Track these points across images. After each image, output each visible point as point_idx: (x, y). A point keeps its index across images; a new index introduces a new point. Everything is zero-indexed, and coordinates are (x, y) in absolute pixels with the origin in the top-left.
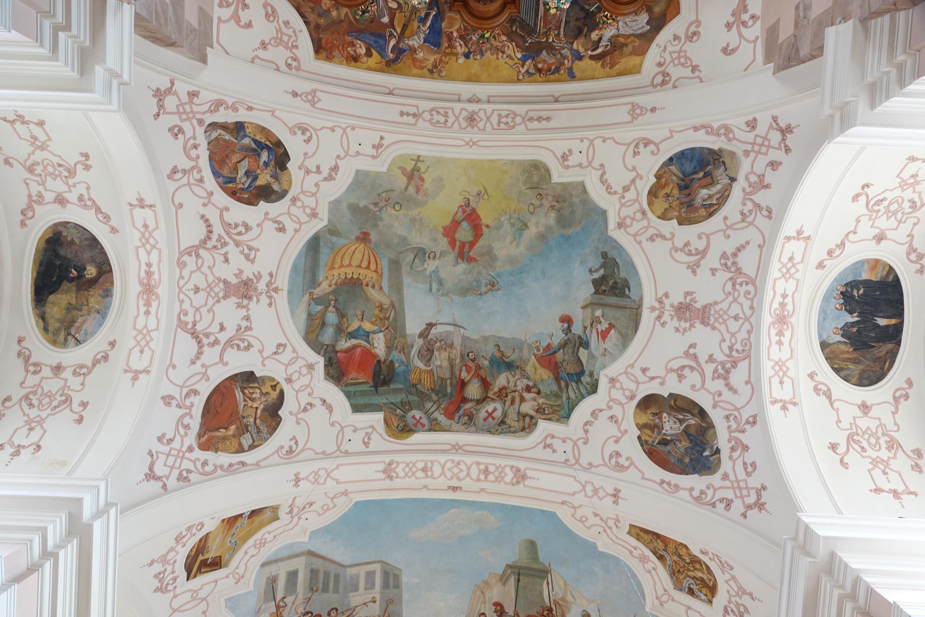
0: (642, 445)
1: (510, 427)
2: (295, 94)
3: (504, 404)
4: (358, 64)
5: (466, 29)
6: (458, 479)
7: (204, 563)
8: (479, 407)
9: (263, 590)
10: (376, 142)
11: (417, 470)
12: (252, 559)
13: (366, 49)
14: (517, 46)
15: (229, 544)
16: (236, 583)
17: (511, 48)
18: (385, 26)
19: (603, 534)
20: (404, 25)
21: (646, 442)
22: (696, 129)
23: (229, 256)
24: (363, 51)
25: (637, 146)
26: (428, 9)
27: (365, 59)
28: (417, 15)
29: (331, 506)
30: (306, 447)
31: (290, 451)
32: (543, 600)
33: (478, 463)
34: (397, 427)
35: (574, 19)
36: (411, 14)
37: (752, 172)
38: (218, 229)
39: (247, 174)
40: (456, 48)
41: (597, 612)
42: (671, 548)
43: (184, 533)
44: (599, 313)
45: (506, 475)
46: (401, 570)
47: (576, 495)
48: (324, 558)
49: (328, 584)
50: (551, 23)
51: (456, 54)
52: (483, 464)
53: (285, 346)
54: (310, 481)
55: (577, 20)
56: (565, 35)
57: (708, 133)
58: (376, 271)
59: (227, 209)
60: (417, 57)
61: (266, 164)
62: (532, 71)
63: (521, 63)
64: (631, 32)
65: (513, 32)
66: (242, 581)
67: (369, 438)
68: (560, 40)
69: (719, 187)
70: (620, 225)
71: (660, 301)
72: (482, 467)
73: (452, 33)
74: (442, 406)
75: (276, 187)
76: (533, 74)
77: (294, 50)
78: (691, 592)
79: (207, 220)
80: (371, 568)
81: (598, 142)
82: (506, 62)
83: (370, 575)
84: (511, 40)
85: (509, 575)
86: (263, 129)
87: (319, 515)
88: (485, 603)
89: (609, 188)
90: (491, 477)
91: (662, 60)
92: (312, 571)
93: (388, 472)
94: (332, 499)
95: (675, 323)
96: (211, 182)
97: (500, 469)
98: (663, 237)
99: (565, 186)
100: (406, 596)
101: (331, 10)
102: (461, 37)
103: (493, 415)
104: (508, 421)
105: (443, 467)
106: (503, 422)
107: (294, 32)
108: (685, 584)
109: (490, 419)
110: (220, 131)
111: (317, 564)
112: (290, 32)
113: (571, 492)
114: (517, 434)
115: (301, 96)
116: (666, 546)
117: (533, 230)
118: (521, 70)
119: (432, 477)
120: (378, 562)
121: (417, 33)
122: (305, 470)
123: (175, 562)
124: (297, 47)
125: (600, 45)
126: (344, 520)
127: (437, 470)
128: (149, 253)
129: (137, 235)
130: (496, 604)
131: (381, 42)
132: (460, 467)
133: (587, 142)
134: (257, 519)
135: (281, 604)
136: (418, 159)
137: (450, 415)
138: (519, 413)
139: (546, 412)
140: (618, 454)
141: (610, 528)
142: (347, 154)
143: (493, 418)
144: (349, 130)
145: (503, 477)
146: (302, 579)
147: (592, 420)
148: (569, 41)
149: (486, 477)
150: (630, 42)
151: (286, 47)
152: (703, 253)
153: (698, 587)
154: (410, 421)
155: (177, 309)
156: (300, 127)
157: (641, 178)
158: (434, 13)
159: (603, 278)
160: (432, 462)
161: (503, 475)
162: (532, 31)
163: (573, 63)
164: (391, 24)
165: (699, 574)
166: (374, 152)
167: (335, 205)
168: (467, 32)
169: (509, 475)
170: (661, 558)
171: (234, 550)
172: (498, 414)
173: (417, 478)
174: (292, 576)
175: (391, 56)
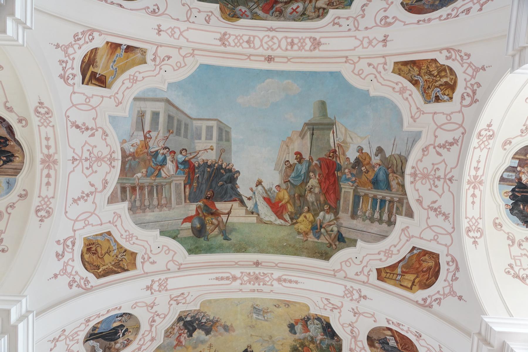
0: (404, 7)
1: (309, 16)
3: (305, 3)
6: (272, 49)
7: (94, 74)
8: (286, 6)
9: (135, 120)
11: (244, 41)
12: (128, 91)
15: (112, 69)
16: (117, 106)
19: (375, 80)
21: (407, 4)
29: (183, 65)
30: (165, 13)
31: (154, 12)
32: (330, 146)
33: (286, 38)
34: (229, 15)
41: (368, 145)
42: (424, 67)
43: (80, 36)
45: (306, 44)
46: (231, 128)
47: (356, 49)
48: (177, 109)
49: (180, 130)
52: (290, 38)
54: (168, 34)
66: (120, 106)
67: (209, 18)
72: (289, 40)
74: (260, 5)
78: (437, 99)
80: (211, 123)
83: (209, 129)
85: (307, 131)
87: (174, 70)
88: (289, 153)
90: (296, 47)
92: (169, 116)
93: (223, 39)
97: (302, 41)
100: (234, 148)
103: (297, 10)
104: (307, 13)
105: (261, 41)
106: (304, 14)
108: (433, 96)
109: (295, 13)
111: (173, 112)
113: (353, 48)
114: (314, 20)
116: (420, 69)
119: (254, 48)
120: (215, 120)
122: (166, 23)
123: (74, 59)
126: (191, 79)
127: (257, 43)
130: (297, 153)
132: (273, 41)
134: (132, 56)
135: (148, 135)
137: (266, 11)
138: (315, 7)
139: (335, 4)
140: (386, 17)
141: (380, 73)
143: (297, 12)
145: (304, 46)
146: (162, 119)
147: (368, 2)
149: (292, 48)
153: (442, 91)
154: (238, 13)
160: (254, 37)
161: (304, 44)
165: (444, 80)
169: (309, 43)
170: (415, 83)
171: (116, 75)
172: (300, 9)
173: (243, 48)
174: (156, 115)
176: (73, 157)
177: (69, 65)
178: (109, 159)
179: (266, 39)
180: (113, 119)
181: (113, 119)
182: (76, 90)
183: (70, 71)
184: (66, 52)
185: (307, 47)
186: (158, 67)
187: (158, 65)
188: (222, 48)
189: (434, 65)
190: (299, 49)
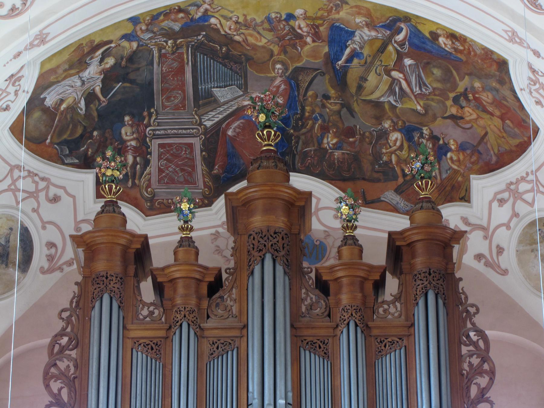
2: (537, 54)
4: (451, 32)
5: (294, 46)
13: (438, 40)
14: (218, 31)
17: (227, 27)
18: (408, 55)
20: (382, 52)
24: (442, 40)
26: (348, 66)
27: (439, 32)
28: (363, 61)
35: (140, 69)
36: (372, 63)
40: (308, 25)
50: (173, 59)
51: (306, 18)
55: (138, 69)
56: (151, 51)
60: (364, 19)
62: (192, 9)
63: (209, 13)
64: (63, 83)
65: (226, 45)
68: (156, 44)
73: (314, 41)
76: (190, 5)
77: (534, 78)
82: (232, 12)
84: (226, 36)
91: (17, 83)
101: (481, 89)
102: (300, 37)
107: (531, 93)
112: (535, 94)
115: (529, 47)
118: (208, 7)
121: (365, 42)
124: (530, 78)
125: (101, 56)
131: (416, 41)
148: (144, 47)
150: (62, 74)
156: (536, 7)
158: (340, 63)
162: (198, 48)
163: (135, 30)
164: (400, 57)
168: (292, 42)
175: (402, 25)
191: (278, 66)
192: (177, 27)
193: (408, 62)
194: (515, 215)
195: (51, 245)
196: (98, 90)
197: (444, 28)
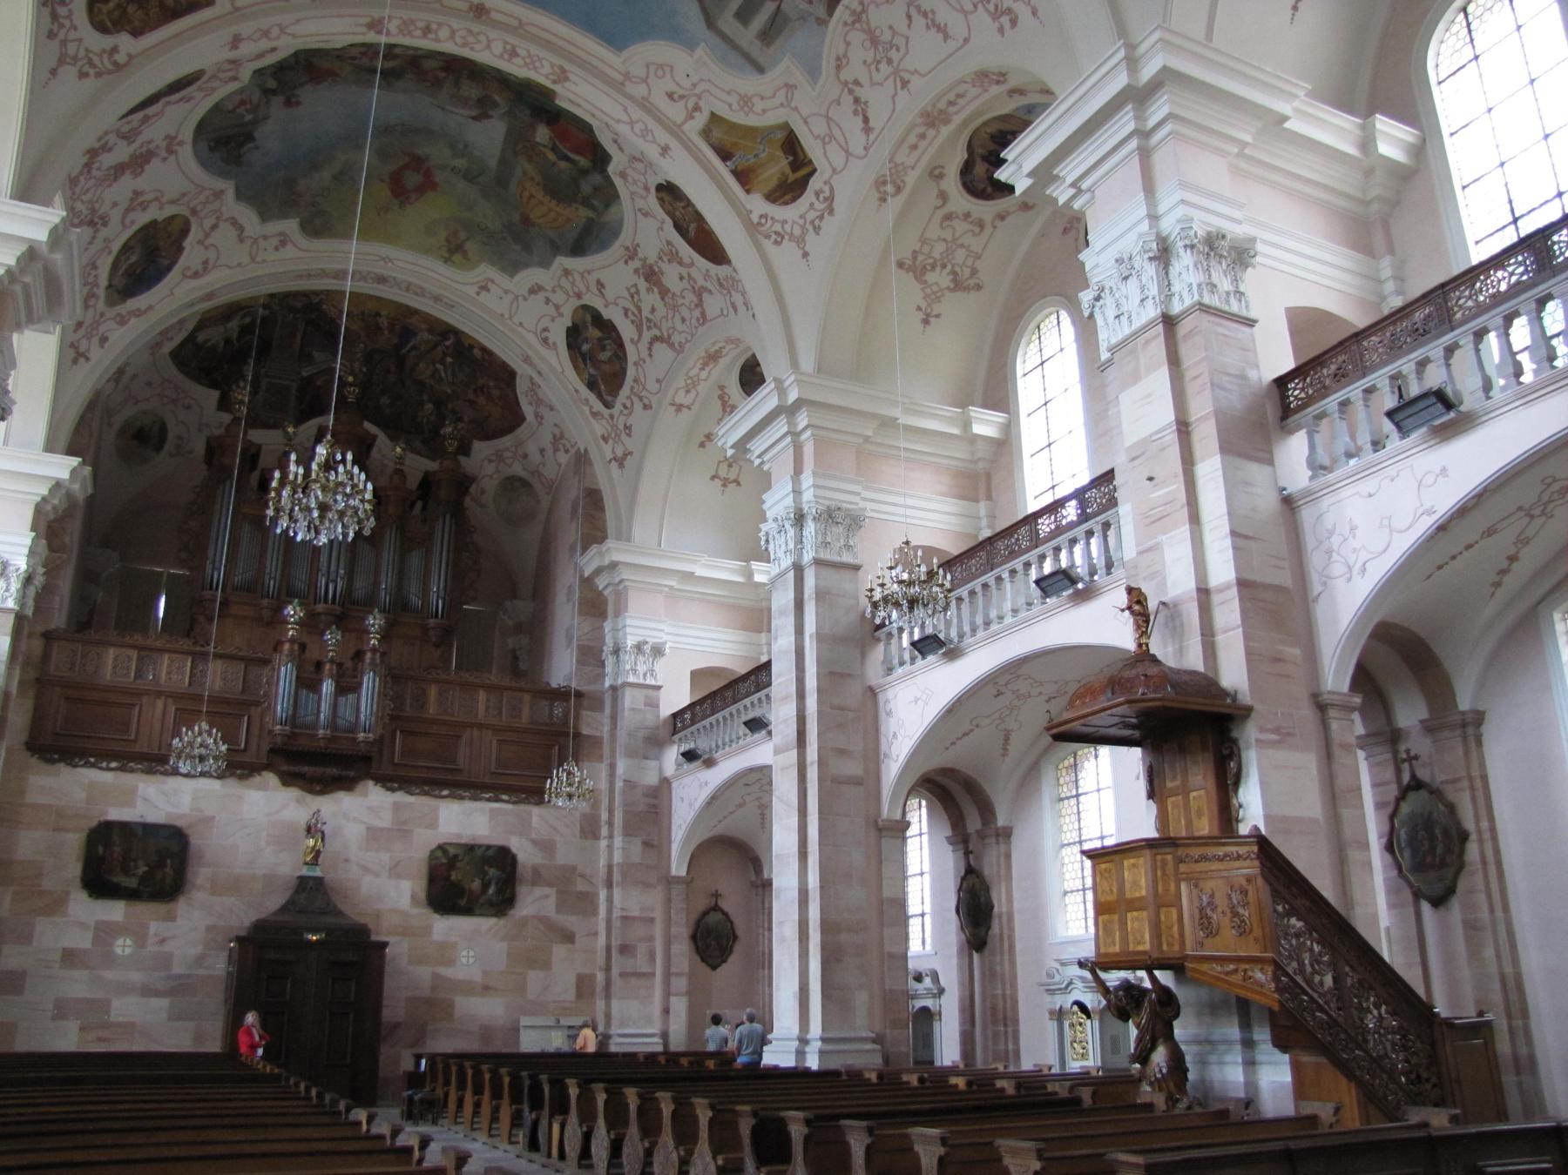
2: (540, 373)
10: (484, 293)
22: (150, 308)
23: (649, 309)
25: (205, 269)
37: (94, 306)
38: (647, 336)
39: (603, 349)
43: (774, 236)
44: (249, 117)
53: (640, 210)
57: (138, 310)
58: (524, 188)
59: (632, 340)
61: (586, 340)
69: (120, 272)
70: (222, 192)
71: (170, 151)
75: (588, 318)
79: (650, 349)
81: (246, 260)
86: (576, 367)
89: (234, 222)
93: (563, 76)
94: (645, 81)
95: (152, 146)
96: (631, 372)
98: (173, 202)
99: (283, 215)
105: (488, 47)
110: (605, 397)
117: (326, 174)
119: (506, 43)
127: (497, 47)
128: (698, 375)
129: (699, 388)
133: (258, 259)
136: (446, 261)
142: (517, 297)
144: (507, 316)
151: (536, 394)
152: (128, 210)
155: (701, 329)
157: (200, 242)
159: (242, 145)
160: (501, 56)
164: (445, 355)
166: (490, 285)
167: (545, 264)
176: (902, 88)
177: (812, 215)
178: (859, 20)
179: (477, 47)
180: (813, 72)
181: (813, 72)
182: (829, 172)
183: (819, 206)
184: (804, 234)
185: (396, 22)
186: (697, 91)
187: (696, 95)
188: (567, 66)
189: (137, 23)
190: (413, 21)
191: (362, 345)
192: (299, 305)
193: (449, 360)
194: (498, 471)
195: (180, 438)
196: (235, 335)
197: (479, 343)
